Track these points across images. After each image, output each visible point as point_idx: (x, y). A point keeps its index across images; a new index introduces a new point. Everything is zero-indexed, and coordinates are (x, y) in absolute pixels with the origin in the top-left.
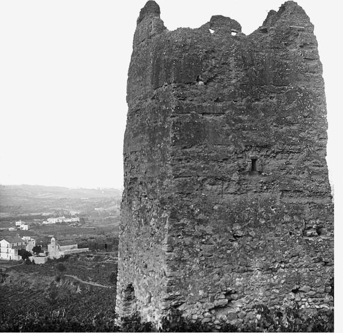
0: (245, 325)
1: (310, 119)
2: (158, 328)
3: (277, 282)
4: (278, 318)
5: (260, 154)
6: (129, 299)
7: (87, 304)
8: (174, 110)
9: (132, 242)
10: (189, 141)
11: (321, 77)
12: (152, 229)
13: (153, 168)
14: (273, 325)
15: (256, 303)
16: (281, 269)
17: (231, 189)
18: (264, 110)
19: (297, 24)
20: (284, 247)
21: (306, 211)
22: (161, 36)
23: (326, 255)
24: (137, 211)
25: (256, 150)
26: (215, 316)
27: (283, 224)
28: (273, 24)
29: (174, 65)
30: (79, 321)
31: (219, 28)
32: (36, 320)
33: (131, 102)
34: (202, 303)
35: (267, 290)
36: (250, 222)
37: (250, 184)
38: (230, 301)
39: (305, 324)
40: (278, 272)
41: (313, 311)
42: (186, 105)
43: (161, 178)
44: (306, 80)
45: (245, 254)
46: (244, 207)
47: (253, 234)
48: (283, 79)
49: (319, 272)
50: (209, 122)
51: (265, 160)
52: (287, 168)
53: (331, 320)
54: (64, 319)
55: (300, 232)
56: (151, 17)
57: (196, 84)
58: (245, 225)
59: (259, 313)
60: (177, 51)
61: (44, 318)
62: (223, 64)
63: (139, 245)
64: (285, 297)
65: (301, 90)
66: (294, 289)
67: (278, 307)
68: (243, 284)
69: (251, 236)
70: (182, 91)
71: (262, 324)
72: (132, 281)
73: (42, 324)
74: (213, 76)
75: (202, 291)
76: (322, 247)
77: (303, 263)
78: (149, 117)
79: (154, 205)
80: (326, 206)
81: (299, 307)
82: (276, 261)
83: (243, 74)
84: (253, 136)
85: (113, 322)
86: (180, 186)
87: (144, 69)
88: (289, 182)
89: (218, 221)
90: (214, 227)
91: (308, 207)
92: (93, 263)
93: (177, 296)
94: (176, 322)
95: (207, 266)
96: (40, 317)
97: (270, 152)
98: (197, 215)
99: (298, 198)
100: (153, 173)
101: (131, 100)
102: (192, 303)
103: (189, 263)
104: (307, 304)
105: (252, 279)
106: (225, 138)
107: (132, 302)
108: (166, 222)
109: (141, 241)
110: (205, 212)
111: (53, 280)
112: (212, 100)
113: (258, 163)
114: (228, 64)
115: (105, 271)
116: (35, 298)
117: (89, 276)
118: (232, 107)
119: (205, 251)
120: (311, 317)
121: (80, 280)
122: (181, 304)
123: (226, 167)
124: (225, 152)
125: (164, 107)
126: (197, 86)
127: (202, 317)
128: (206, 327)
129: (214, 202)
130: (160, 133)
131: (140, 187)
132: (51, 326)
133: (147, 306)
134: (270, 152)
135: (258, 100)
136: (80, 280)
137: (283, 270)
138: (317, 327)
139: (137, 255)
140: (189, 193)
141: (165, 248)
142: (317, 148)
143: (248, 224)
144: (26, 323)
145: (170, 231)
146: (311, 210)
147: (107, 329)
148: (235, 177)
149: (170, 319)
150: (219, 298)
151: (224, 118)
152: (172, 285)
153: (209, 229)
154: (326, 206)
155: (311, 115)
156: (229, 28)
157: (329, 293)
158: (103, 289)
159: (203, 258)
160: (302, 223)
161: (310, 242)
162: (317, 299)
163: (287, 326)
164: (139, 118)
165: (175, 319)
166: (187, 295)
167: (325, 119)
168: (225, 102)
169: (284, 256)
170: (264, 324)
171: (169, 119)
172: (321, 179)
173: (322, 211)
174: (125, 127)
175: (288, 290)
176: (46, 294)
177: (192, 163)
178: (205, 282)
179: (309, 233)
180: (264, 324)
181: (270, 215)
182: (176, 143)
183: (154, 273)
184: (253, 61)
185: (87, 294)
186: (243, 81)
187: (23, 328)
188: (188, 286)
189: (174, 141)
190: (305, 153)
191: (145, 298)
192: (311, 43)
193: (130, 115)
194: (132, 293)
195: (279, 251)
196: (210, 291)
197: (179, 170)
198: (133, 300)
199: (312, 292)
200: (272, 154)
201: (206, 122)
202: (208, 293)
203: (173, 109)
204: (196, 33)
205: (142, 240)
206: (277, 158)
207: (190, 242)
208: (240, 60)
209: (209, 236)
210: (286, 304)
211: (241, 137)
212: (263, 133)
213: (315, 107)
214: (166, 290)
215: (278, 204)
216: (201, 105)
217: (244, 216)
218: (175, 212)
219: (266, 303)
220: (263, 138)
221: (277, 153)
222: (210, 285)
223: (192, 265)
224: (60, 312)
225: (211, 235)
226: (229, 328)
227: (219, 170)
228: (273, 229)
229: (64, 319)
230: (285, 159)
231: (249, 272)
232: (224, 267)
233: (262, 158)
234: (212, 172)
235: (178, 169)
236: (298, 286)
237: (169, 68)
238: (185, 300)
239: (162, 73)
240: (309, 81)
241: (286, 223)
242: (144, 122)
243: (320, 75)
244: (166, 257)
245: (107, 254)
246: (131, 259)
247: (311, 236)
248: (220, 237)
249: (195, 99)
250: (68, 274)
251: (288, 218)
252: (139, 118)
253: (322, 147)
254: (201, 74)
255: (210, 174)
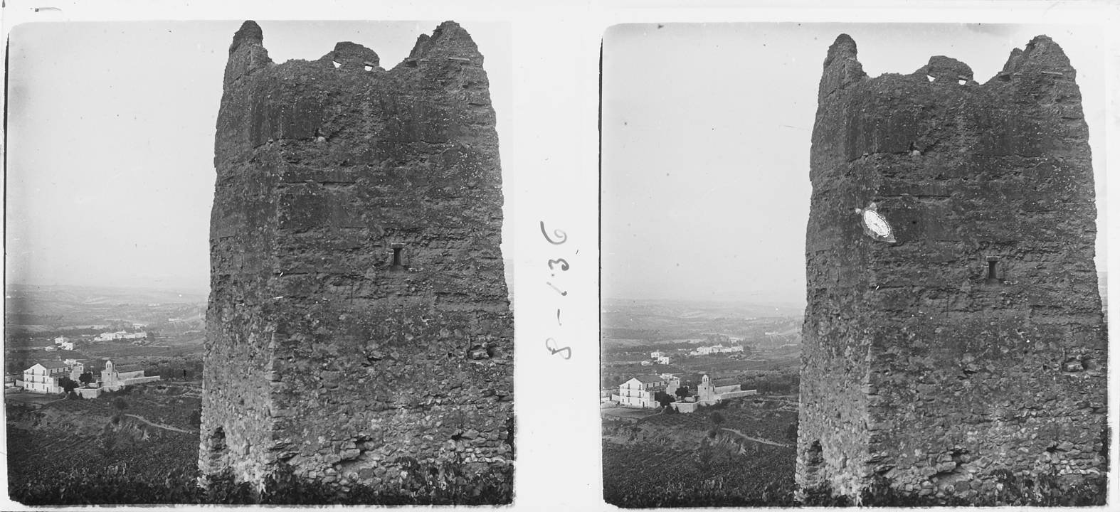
0: (384, 486)
1: (478, 190)
2: (260, 491)
3: (430, 424)
4: (431, 476)
5: (407, 241)
6: (218, 449)
7: (158, 456)
8: (283, 177)
9: (223, 367)
10: (305, 223)
11: (494, 130)
12: (251, 348)
13: (253, 261)
14: (425, 486)
15: (400, 455)
16: (436, 407)
17: (364, 291)
18: (411, 178)
19: (460, 55)
20: (440, 374)
21: (472, 322)
22: (264, 72)
23: (501, 386)
24: (230, 322)
25: (400, 235)
26: (342, 473)
27: (439, 341)
28: (424, 55)
29: (283, 114)
30: (146, 480)
31: (348, 60)
32: (85, 479)
33: (221, 166)
34: (322, 454)
35: (415, 437)
36: (391, 338)
37: (391, 284)
38: (362, 452)
39: (471, 485)
40: (432, 410)
41: (482, 467)
42: (300, 170)
43: (264, 275)
44: (472, 135)
45: (385, 384)
46: (384, 317)
47: (396, 355)
48: (439, 133)
49: (490, 411)
50: (332, 195)
51: (413, 250)
52: (445, 262)
53: (508, 479)
54: (125, 477)
55: (463, 353)
56: (250, 44)
57: (315, 141)
58: (384, 343)
59: (404, 469)
60: (287, 93)
61: (96, 476)
62: (353, 112)
63: (232, 371)
64: (441, 446)
65: (465, 149)
66: (454, 434)
67: (432, 460)
68: (382, 427)
69: (393, 359)
70: (294, 151)
71: (409, 485)
72: (222, 424)
73: (93, 485)
74: (338, 130)
75: (323, 437)
76: (494, 375)
77: (468, 398)
78: (247, 189)
79: (254, 314)
80: (501, 315)
81: (462, 460)
82: (429, 395)
83: (381, 126)
84: (396, 215)
85: (195, 482)
86: (292, 287)
87: (239, 119)
88: (448, 281)
89: (346, 337)
90: (340, 345)
91: (474, 317)
92: (166, 397)
93: (287, 444)
94: (285, 481)
95: (331, 402)
96: (91, 475)
97: (420, 238)
98: (316, 328)
99: (461, 304)
100: (252, 268)
101: (221, 164)
102: (308, 455)
103: (304, 397)
104: (473, 456)
105: (395, 420)
106: (355, 218)
107: (222, 453)
108: (271, 339)
109: (236, 366)
110: (327, 325)
111: (109, 421)
112: (336, 163)
113: (403, 254)
114: (360, 112)
115: (184, 409)
116: (83, 447)
117: (162, 416)
118: (366, 173)
119: (328, 381)
120: (479, 475)
121: (148, 422)
122: (293, 457)
123: (357, 260)
124: (355, 237)
125: (268, 174)
126: (315, 143)
127: (323, 475)
128: (329, 489)
129: (340, 310)
130: (263, 211)
131: (234, 288)
132: (107, 488)
133: (243, 459)
134: (420, 238)
135: (404, 164)
136: (148, 422)
137: (439, 407)
138: (487, 488)
139: (229, 386)
140: (305, 297)
141: (269, 376)
142: (487, 232)
143: (389, 342)
144: (70, 484)
145: (276, 351)
146: (479, 321)
147: (187, 492)
148: (370, 274)
149: (277, 477)
150: (347, 447)
151: (354, 189)
152: (279, 428)
153: (332, 348)
154: (501, 315)
155: (479, 185)
156: (362, 60)
157: (506, 440)
158: (180, 435)
159: (324, 391)
160: (467, 340)
161: (478, 368)
162: (488, 449)
163: (444, 488)
164: (232, 189)
165: (283, 478)
166: (301, 444)
167: (499, 191)
168: (355, 166)
169: (441, 387)
170: (412, 485)
171: (275, 191)
172: (493, 277)
173: (495, 322)
174: (213, 203)
175: (445, 436)
176: (98, 443)
177: (309, 254)
178: (327, 425)
179: (476, 354)
180: (412, 485)
181: (420, 328)
182: (286, 225)
183: (253, 412)
184: (395, 107)
185: (158, 441)
186: (381, 135)
187: (65, 491)
188: (303, 430)
189: (282, 222)
190: (471, 240)
191: (241, 448)
192: (480, 82)
193: (220, 185)
194: (222, 440)
195: (433, 380)
196: (334, 438)
197: (290, 264)
198: (224, 451)
199: (480, 438)
200: (424, 241)
201: (329, 194)
202: (332, 440)
203: (280, 176)
204: (313, 68)
205: (236, 363)
206: (430, 246)
207: (305, 367)
208: (377, 105)
209: (333, 359)
210: (444, 456)
211: (378, 216)
212: (410, 211)
213: (485, 173)
214: (271, 436)
215: (432, 312)
216: (322, 171)
217: (383, 330)
218: (284, 325)
219: (415, 455)
220: (410, 218)
221: (430, 240)
222: (334, 429)
223: (308, 400)
224: (119, 467)
225: (336, 357)
226: (361, 491)
227: (348, 264)
228: (425, 348)
229: (125, 477)
230: (442, 248)
231: (390, 411)
232: (355, 404)
233: (409, 246)
234: (337, 267)
235: (288, 263)
236: (460, 431)
237: (276, 117)
238: (298, 450)
239: (266, 125)
240: (476, 135)
241: (443, 339)
242: (239, 195)
243: (492, 128)
244: (271, 389)
245: (186, 385)
246: (220, 391)
247: (480, 358)
248: (348, 361)
249: (313, 161)
250: (130, 413)
251: (446, 332)
252: (232, 189)
253: (496, 231)
254: (321, 126)
255: (335, 270)
